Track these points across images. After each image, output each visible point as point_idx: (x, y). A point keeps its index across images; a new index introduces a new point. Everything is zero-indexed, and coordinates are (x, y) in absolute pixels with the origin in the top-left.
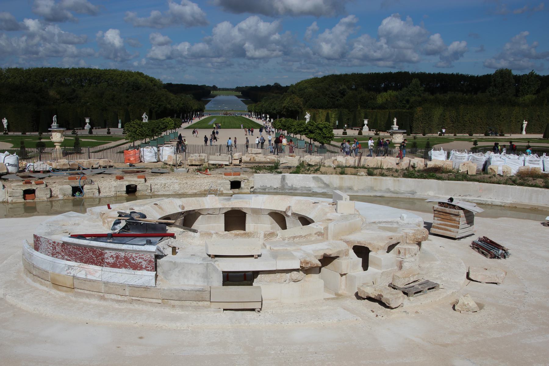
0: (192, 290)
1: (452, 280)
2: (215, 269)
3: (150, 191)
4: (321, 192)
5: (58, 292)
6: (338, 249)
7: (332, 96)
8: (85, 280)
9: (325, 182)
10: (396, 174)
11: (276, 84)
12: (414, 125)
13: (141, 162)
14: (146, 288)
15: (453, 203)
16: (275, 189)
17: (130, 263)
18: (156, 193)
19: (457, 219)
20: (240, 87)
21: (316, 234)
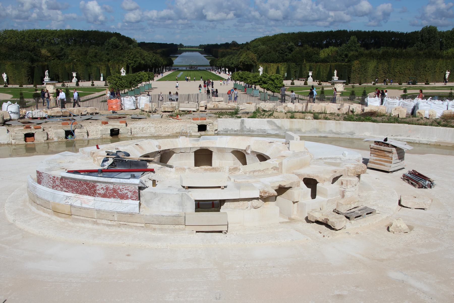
2: (189, 198)
3: (130, 134)
4: (274, 133)
5: (58, 218)
6: (291, 181)
7: (281, 52)
8: (81, 208)
9: (278, 125)
10: (338, 118)
11: (233, 42)
12: (352, 76)
13: (122, 109)
14: (132, 214)
15: (387, 142)
16: (235, 131)
18: (135, 135)
19: (390, 155)
20: (203, 45)
21: (272, 168)
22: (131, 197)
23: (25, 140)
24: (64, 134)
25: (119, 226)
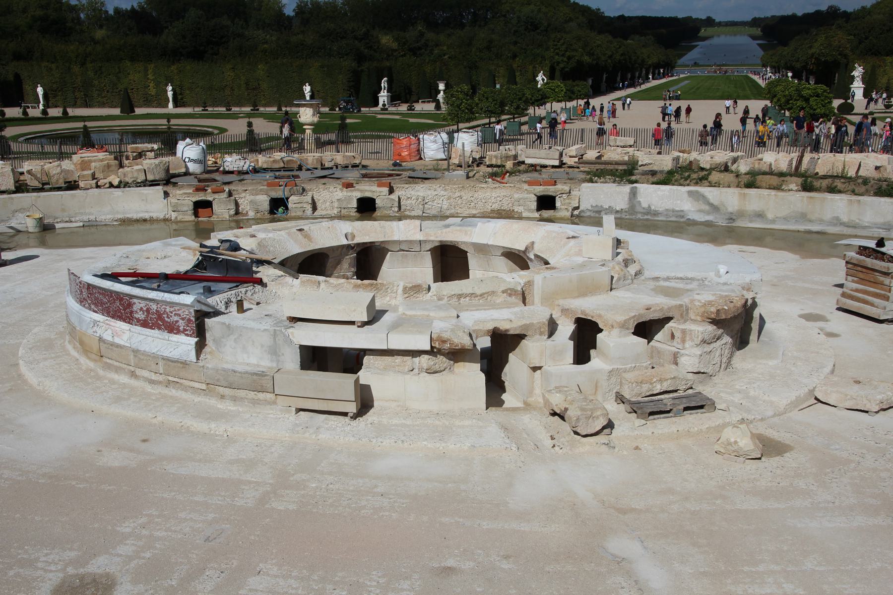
0: (247, 373)
1: (766, 398)
2: (289, 341)
3: (396, 209)
4: (703, 220)
5: (87, 361)
6: (524, 322)
8: (113, 344)
9: (712, 201)
10: (863, 189)
11: (831, 7)
13: (421, 159)
14: (185, 364)
15: (883, 250)
16: (617, 212)
17: (163, 320)
18: (407, 213)
19: (887, 281)
20: (760, 19)
21: (503, 292)
22: (185, 330)
23: (196, 214)
24: (266, 206)
25: (168, 384)
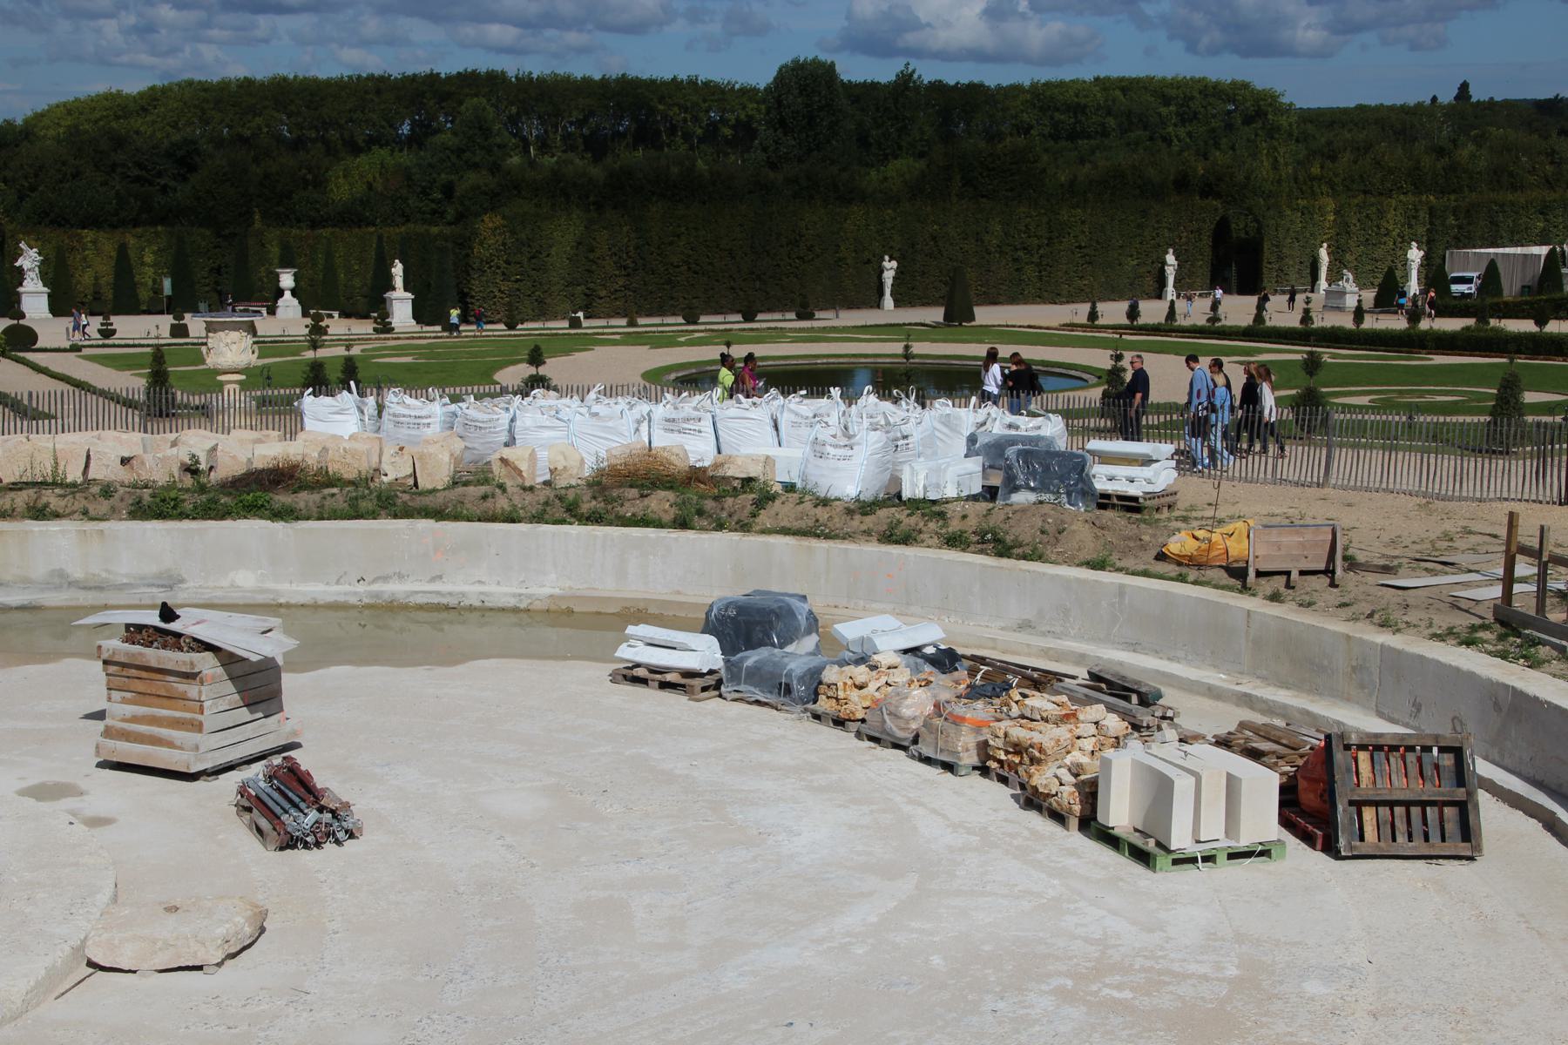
7: (136, 172)
12: (476, 286)
15: (174, 626)
19: (192, 690)
